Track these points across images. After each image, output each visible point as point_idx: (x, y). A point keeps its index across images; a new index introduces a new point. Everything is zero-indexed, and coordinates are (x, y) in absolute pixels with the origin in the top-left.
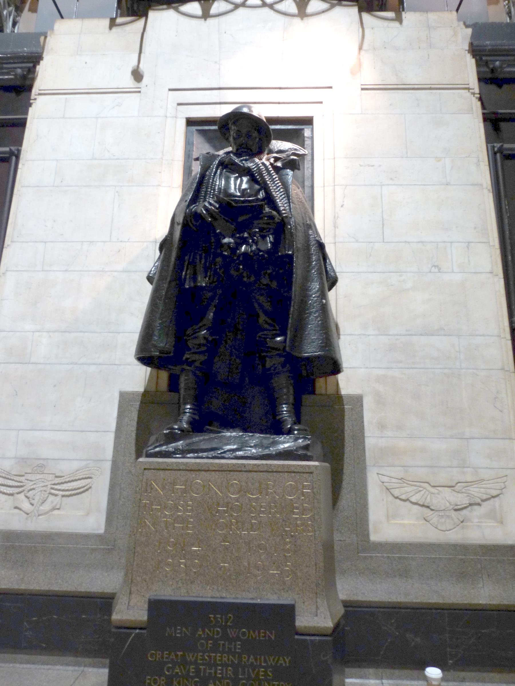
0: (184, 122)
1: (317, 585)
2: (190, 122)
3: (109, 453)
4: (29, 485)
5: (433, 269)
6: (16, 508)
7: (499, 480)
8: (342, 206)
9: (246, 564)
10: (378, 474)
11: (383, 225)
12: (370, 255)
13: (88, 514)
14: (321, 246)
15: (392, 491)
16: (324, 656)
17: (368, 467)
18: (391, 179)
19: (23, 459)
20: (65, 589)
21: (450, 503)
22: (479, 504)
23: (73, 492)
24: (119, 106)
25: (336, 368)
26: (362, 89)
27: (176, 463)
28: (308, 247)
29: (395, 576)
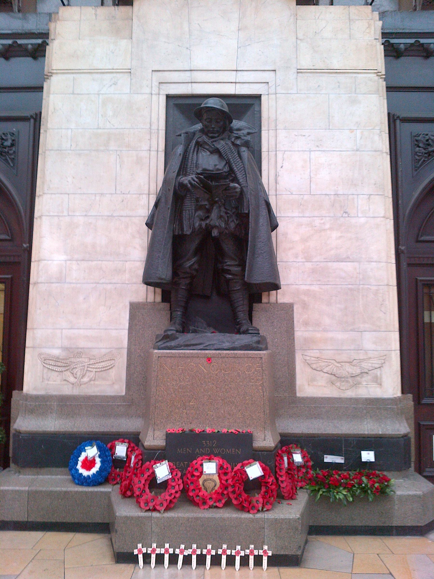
0: (165, 97)
1: (265, 423)
4: (72, 366)
5: (345, 215)
6: (65, 380)
7: (381, 358)
8: (282, 167)
9: (223, 412)
10: (303, 355)
11: (310, 181)
12: (301, 204)
13: (114, 383)
14: (268, 205)
15: (312, 366)
16: (269, 462)
17: (296, 351)
18: (317, 146)
19: (67, 348)
20: (102, 430)
21: (348, 372)
22: (367, 373)
23: (103, 369)
24: (115, 84)
25: (276, 287)
26: (298, 72)
27: (178, 353)
28: (258, 206)
29: (312, 418)
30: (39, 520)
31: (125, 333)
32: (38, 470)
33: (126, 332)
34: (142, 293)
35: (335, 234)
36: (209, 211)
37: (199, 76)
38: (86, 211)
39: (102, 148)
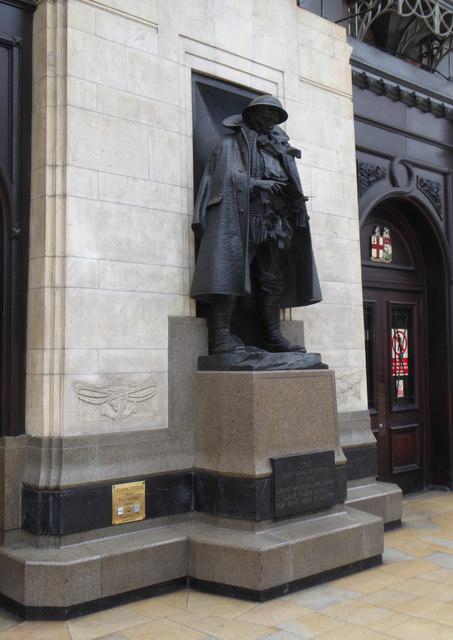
2: (194, 73)
3: (166, 369)
30: (114, 593)
31: (165, 353)
32: (82, 534)
33: (166, 351)
34: (184, 308)
35: (329, 254)
36: (274, 220)
37: (224, 58)
38: (119, 198)
39: (132, 119)
